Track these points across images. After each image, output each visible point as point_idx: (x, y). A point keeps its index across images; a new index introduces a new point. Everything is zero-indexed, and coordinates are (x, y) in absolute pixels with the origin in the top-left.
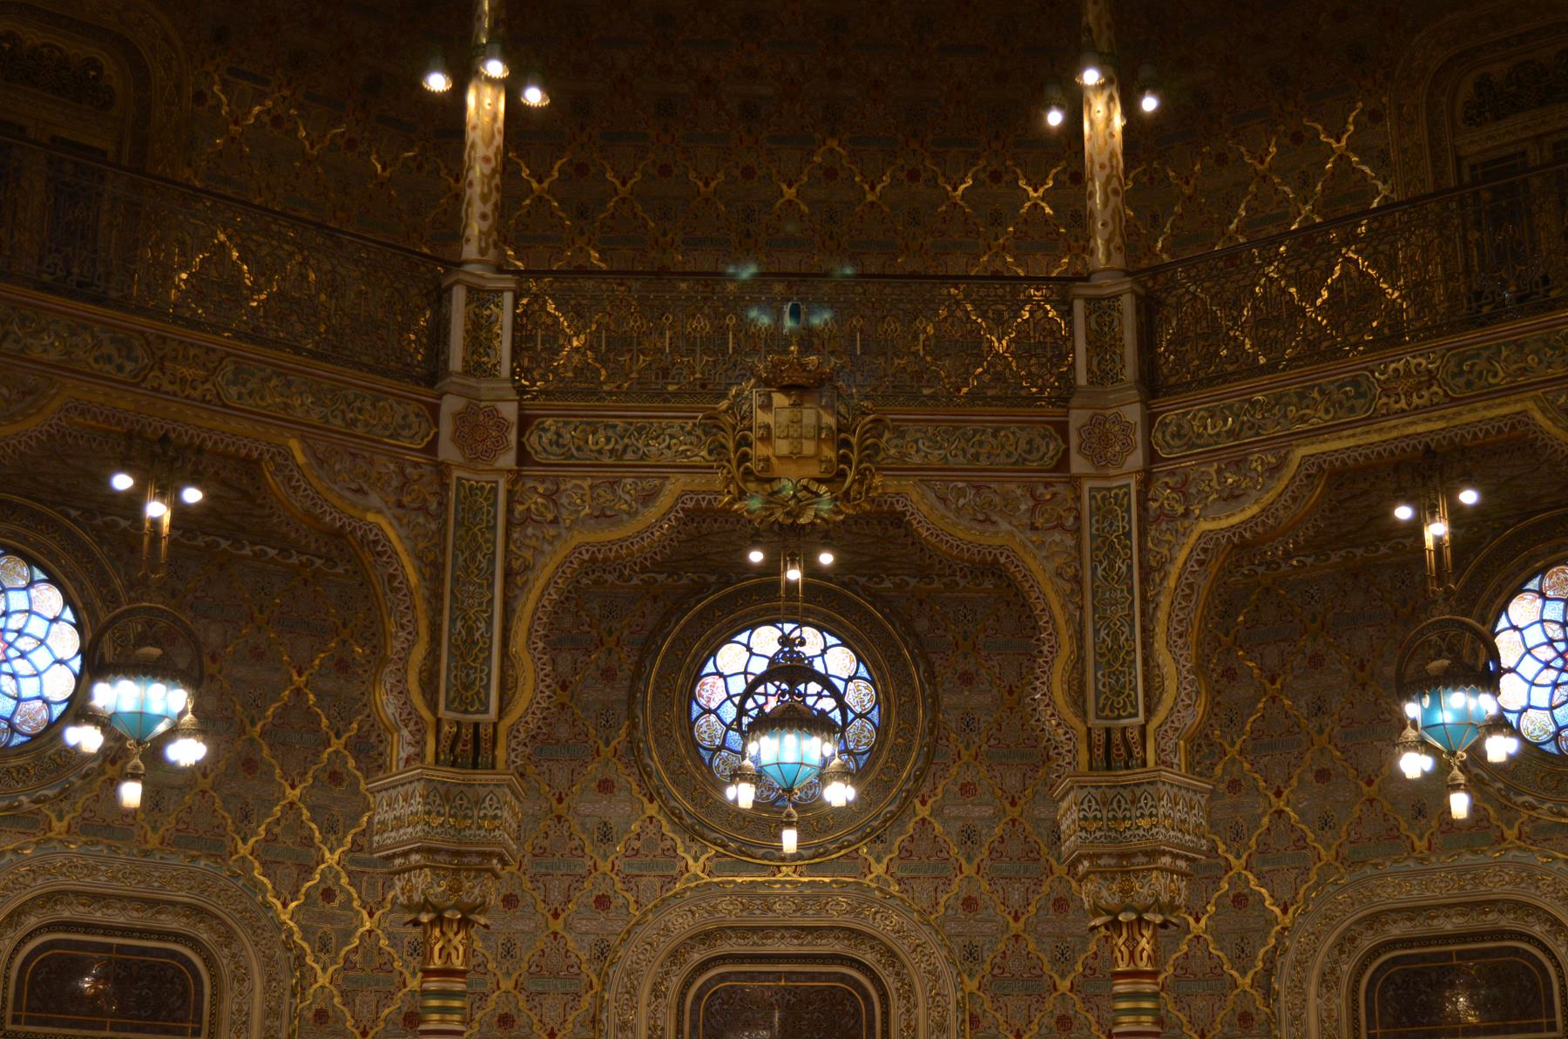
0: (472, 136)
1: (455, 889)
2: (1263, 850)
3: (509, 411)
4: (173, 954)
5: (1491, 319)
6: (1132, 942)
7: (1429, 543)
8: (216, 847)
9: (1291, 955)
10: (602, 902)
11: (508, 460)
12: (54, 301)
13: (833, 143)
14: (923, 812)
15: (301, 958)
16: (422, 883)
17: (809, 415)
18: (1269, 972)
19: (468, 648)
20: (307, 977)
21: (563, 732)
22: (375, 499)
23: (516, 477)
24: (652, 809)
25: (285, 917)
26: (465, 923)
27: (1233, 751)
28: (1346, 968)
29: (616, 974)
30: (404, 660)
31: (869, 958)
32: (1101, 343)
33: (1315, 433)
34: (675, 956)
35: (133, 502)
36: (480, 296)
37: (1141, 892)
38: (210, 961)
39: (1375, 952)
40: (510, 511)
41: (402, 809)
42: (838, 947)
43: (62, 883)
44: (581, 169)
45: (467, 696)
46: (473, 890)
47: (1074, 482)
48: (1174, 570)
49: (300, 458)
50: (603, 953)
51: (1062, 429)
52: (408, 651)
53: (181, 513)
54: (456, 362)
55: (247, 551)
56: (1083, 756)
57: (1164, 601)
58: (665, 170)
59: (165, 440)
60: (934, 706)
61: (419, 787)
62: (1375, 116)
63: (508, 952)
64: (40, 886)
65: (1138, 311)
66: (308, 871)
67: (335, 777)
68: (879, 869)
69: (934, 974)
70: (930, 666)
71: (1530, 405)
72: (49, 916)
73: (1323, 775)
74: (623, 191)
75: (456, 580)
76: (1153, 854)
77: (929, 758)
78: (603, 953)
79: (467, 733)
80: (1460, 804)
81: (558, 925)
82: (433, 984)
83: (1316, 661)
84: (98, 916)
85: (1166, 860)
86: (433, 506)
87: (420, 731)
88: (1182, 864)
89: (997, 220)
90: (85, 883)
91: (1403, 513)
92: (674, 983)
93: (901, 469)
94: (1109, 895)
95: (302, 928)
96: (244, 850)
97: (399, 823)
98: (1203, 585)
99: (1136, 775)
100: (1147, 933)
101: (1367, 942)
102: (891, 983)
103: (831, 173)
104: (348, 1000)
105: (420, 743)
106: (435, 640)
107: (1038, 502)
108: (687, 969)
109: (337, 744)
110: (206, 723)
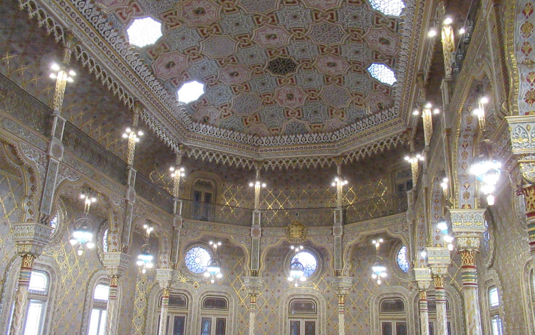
0: (256, 192)
1: (254, 291)
3: (260, 229)
6: (341, 299)
8: (228, 284)
11: (260, 236)
12: (202, 222)
15: (240, 299)
16: (250, 291)
17: (298, 229)
19: (255, 260)
21: (274, 268)
22: (242, 242)
23: (261, 238)
25: (237, 293)
28: (379, 301)
29: (280, 301)
31: (314, 299)
32: (338, 217)
34: (288, 298)
35: (213, 245)
36: (256, 214)
38: (227, 299)
39: (382, 299)
40: (260, 242)
42: (310, 297)
43: (208, 290)
45: (255, 267)
46: (256, 292)
47: (334, 236)
51: (332, 229)
53: (218, 246)
54: (253, 223)
56: (334, 274)
60: (323, 264)
62: (384, 178)
63: (267, 298)
64: (206, 290)
65: (343, 212)
68: (316, 286)
70: (323, 258)
71: (387, 229)
74: (281, 192)
77: (322, 271)
79: (255, 272)
81: (273, 294)
82: (251, 304)
84: (213, 294)
90: (211, 290)
91: (374, 242)
92: (288, 302)
94: (337, 293)
95: (240, 295)
96: (232, 285)
100: (343, 298)
101: (381, 298)
102: (317, 302)
103: (310, 188)
104: (246, 304)
105: (249, 273)
107: (329, 239)
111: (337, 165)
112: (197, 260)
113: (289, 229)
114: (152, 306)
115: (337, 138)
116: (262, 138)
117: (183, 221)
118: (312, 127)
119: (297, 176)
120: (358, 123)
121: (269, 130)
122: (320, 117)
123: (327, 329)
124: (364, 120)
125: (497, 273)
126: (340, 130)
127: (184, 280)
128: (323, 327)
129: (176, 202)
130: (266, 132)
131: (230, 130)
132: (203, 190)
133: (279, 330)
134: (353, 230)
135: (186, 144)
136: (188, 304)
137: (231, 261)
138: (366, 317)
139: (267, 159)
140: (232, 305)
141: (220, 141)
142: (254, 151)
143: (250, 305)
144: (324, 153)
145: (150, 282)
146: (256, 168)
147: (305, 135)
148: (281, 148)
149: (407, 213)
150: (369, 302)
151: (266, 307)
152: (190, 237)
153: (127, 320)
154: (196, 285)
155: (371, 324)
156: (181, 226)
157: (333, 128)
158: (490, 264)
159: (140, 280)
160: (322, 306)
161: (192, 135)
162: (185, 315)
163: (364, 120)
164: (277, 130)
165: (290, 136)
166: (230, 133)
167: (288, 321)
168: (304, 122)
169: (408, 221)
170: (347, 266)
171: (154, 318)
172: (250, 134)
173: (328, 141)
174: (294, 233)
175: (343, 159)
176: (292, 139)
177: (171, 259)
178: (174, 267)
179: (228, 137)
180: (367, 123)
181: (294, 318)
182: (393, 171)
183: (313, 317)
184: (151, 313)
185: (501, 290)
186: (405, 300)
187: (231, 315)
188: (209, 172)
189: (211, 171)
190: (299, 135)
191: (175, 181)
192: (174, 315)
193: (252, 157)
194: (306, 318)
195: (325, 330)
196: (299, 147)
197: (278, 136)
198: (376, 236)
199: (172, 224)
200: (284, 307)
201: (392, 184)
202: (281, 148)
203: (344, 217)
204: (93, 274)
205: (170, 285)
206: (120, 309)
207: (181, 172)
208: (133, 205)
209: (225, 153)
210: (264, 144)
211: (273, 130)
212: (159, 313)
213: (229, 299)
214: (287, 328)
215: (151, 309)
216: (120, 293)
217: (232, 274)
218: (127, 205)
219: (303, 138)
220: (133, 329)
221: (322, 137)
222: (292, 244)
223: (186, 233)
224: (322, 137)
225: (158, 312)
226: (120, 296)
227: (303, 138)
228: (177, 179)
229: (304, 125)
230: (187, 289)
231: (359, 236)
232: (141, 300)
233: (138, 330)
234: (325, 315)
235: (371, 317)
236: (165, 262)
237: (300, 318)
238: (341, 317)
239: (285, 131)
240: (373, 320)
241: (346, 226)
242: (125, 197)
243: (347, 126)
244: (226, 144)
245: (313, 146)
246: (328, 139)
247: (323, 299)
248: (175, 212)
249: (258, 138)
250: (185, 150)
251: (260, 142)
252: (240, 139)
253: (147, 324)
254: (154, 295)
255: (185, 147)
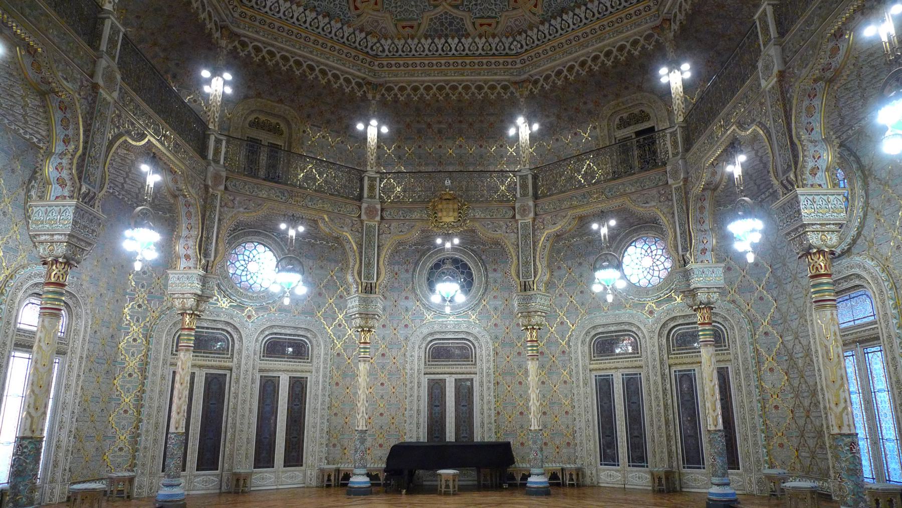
0: (369, 140)
2: (568, 311)
3: (378, 207)
4: (302, 340)
5: (617, 178)
7: (602, 235)
8: (312, 314)
9: (574, 337)
10: (406, 326)
11: (378, 218)
13: (461, 139)
14: (484, 303)
15: (333, 341)
17: (451, 206)
18: (569, 341)
19: (369, 265)
20: (335, 345)
22: (345, 229)
23: (380, 224)
24: (418, 303)
26: (369, 331)
27: (560, 287)
28: (588, 339)
29: (410, 344)
30: (353, 268)
31: (471, 339)
32: (524, 186)
33: (575, 207)
34: (424, 339)
36: (372, 179)
37: (533, 321)
38: (310, 342)
39: (595, 335)
40: (379, 231)
41: (354, 304)
42: (464, 336)
43: (274, 323)
44: (399, 147)
47: (517, 221)
48: (541, 242)
49: (327, 220)
50: (406, 339)
51: (514, 208)
52: (354, 266)
54: (365, 195)
55: (318, 242)
56: (519, 288)
57: (538, 250)
58: (420, 147)
59: (293, 215)
60: (487, 277)
61: (357, 298)
62: (595, 128)
64: (269, 324)
66: (334, 319)
67: (341, 297)
68: (474, 317)
69: (487, 342)
72: (271, 332)
73: (582, 292)
75: (366, 248)
76: (536, 312)
77: (486, 290)
78: (406, 339)
80: (610, 298)
81: (395, 332)
82: (362, 346)
83: (580, 264)
84: (283, 331)
85: (539, 313)
86: (360, 230)
87: (357, 285)
88: (544, 314)
89: (502, 157)
90: (280, 323)
91: (595, 226)
92: (424, 345)
93: (474, 219)
96: (319, 315)
97: (353, 307)
98: (548, 245)
99: (532, 293)
101: (593, 333)
102: (476, 345)
103: (461, 146)
104: (345, 350)
106: (361, 263)
108: (427, 342)
109: (341, 289)
110: (305, 282)
111: (519, 97)
112: (252, 267)
113: (434, 207)
114: (158, 351)
115: (522, 47)
116: (383, 41)
117: (227, 178)
118: (477, 25)
119: (440, 122)
120: (565, 17)
121: (396, 25)
122: (493, 7)
123: (494, 392)
124: (577, 11)
125: (873, 260)
126: (529, 33)
127: (224, 303)
128: (489, 388)
129: (212, 138)
130: (392, 29)
131: (324, 17)
132: (266, 138)
133: (408, 395)
134: (554, 208)
135: (236, 30)
136: (233, 350)
137: (317, 272)
138: (564, 367)
139: (390, 82)
140: (320, 351)
141: (304, 35)
142: (367, 65)
143: (360, 348)
144: (496, 74)
145: (155, 304)
146: (370, 96)
147: (463, 40)
148: (418, 62)
149: (668, 168)
150: (568, 343)
151: (383, 355)
152: (241, 209)
153: (101, 380)
154: (250, 314)
155: (574, 379)
156: (222, 187)
157: (516, 29)
158: (846, 248)
159: (132, 300)
160: (484, 350)
161: (249, 13)
162: (228, 372)
163: (577, 11)
164: (412, 27)
165: (436, 40)
166: (323, 21)
167: (425, 380)
168: (464, 13)
169: (670, 181)
170: (543, 274)
171: (163, 378)
172: (361, 31)
173: (504, 52)
174: (445, 213)
175: (531, 86)
176: (440, 47)
177: (200, 250)
178: (205, 268)
179: (320, 30)
180: (582, 16)
181: (434, 374)
182: (611, 115)
183: (468, 370)
184: (155, 367)
185: (890, 289)
186: (640, 335)
187: (318, 371)
188: (278, 102)
189: (281, 101)
190: (453, 38)
191: (211, 98)
192: (205, 371)
193: (365, 76)
194: (456, 374)
195: (492, 394)
196: (451, 62)
197: (413, 39)
198: (602, 216)
199: (204, 181)
200: (416, 354)
201: (610, 138)
202: (418, 62)
203: (535, 187)
204: (16, 271)
205: (198, 305)
206: (84, 356)
207: (226, 83)
208: (112, 101)
209: (313, 60)
210: (387, 52)
211: (404, 27)
212: (172, 368)
213: (314, 342)
214: (422, 392)
215: (156, 359)
216: (87, 322)
217: (320, 294)
218: (96, 97)
219: (460, 44)
220: (115, 400)
221: (494, 46)
222: (439, 236)
223: (233, 201)
224: (494, 46)
225: (172, 364)
226: (86, 327)
227: (460, 44)
228: (215, 95)
229: (462, 19)
230: (231, 321)
231: (568, 217)
232: (135, 340)
233: (127, 400)
234: (491, 367)
235: (573, 368)
236: (187, 257)
237: (445, 374)
238: (532, 366)
239: (427, 31)
240: (577, 373)
241: (539, 201)
242: (92, 76)
243: (542, 23)
244: (316, 42)
245: (476, 61)
246: (504, 49)
247: (488, 338)
248: (210, 156)
249: (375, 40)
250: (234, 41)
251: (378, 48)
252: (342, 38)
253: (148, 388)
254: (163, 331)
255: (233, 36)
